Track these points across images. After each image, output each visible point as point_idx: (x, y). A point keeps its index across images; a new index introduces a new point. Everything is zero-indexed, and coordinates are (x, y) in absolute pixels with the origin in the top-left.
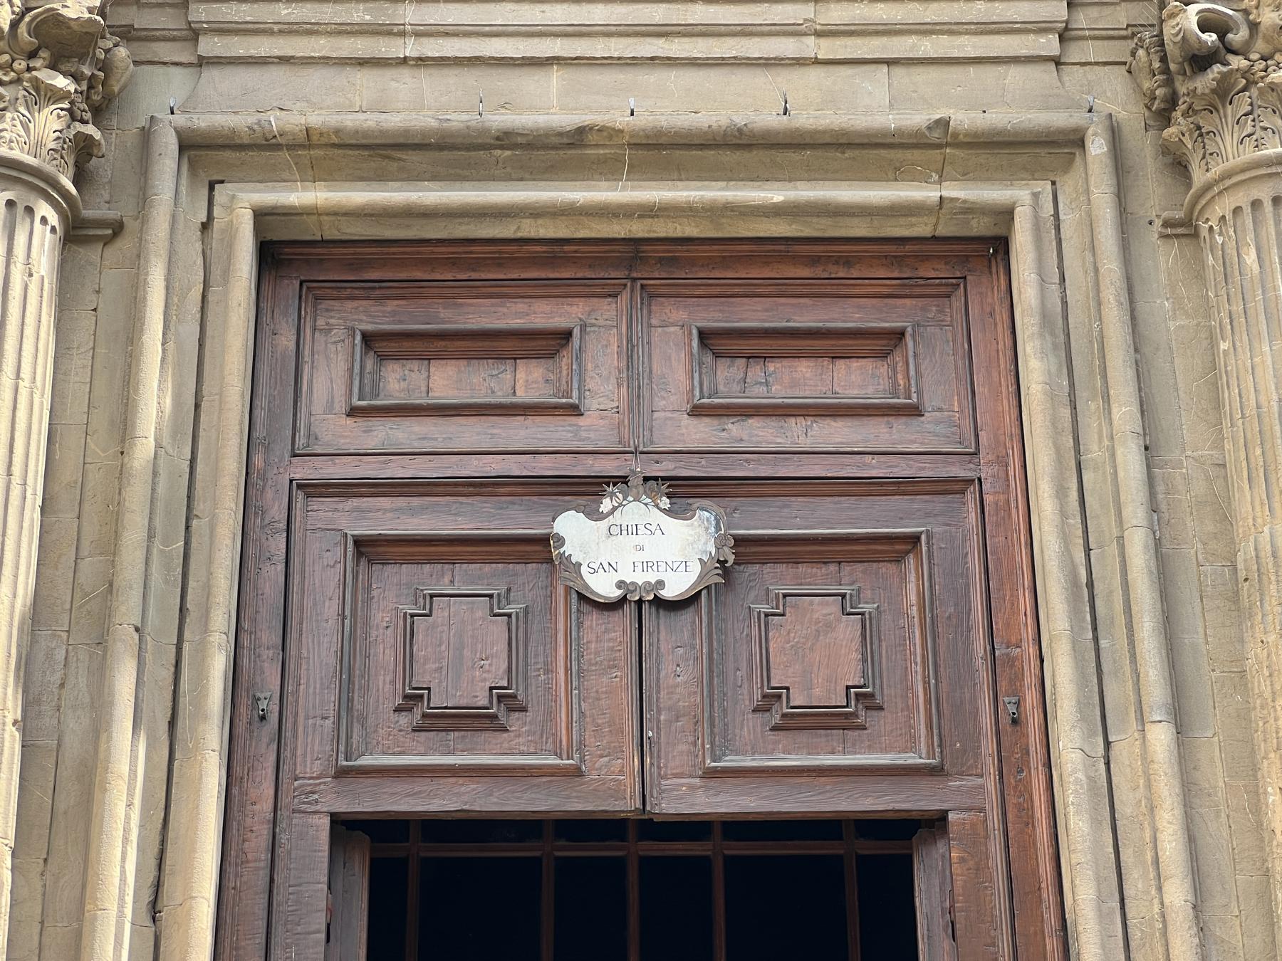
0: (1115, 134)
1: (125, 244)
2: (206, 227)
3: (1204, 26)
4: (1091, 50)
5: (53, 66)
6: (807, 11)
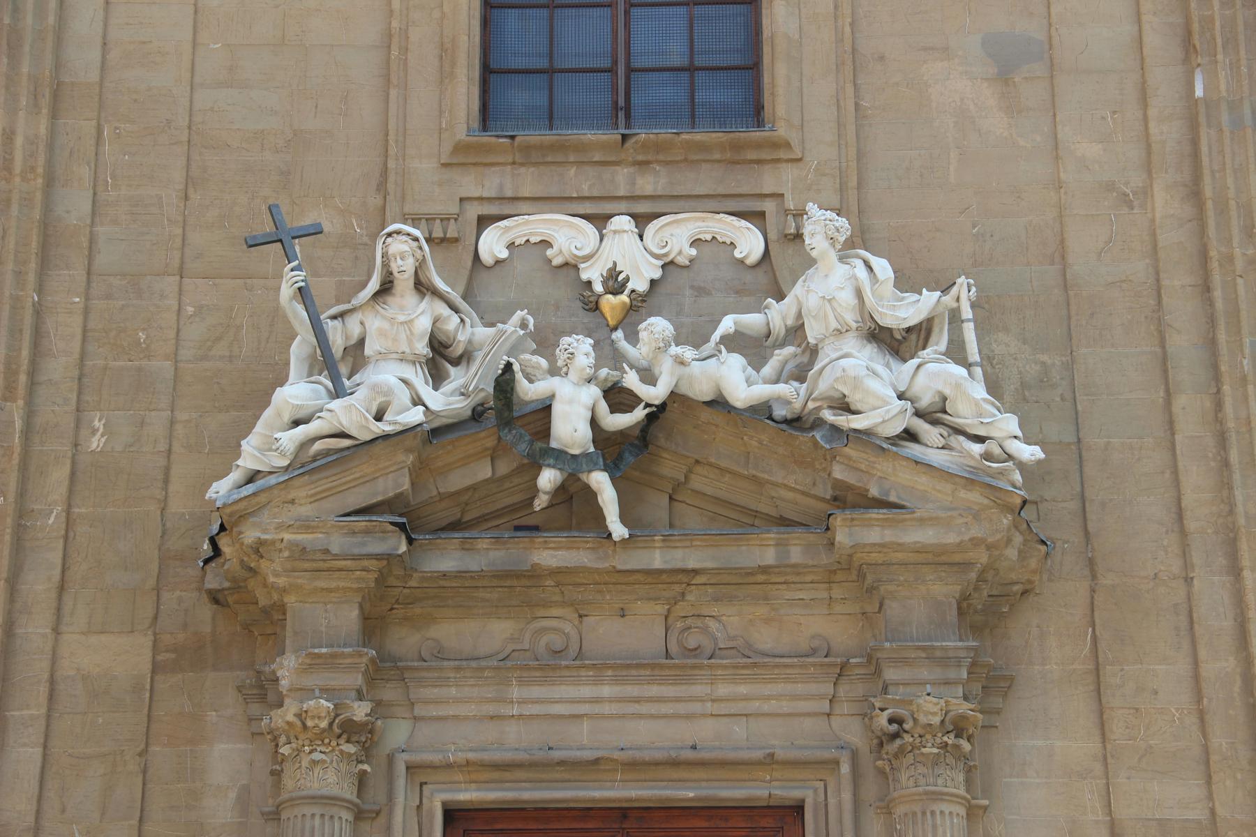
0: (855, 756)
1: (382, 820)
2: (419, 807)
3: (891, 721)
5: (348, 741)
6: (707, 689)
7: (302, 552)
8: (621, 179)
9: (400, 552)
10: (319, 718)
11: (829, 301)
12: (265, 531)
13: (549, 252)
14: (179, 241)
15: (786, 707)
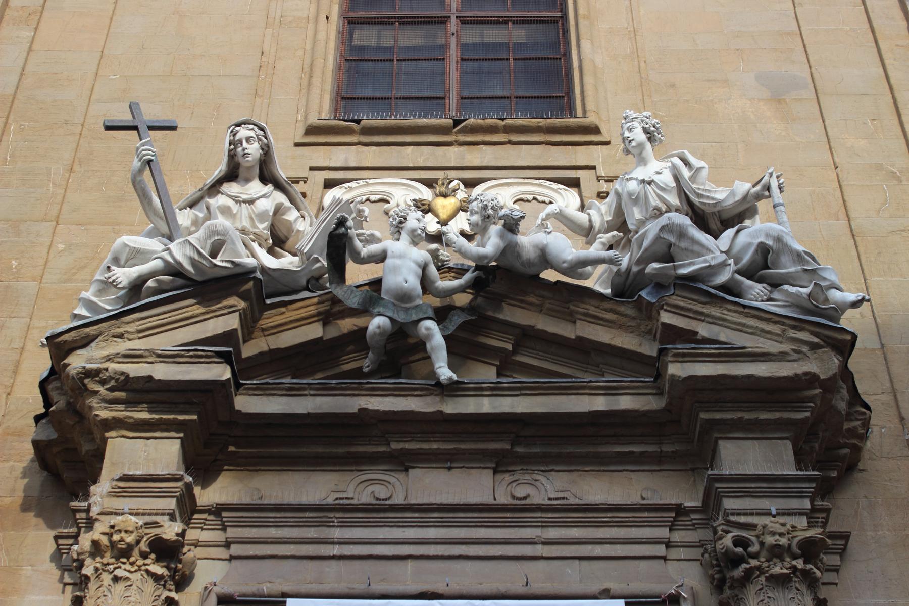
0: (694, 596)
4: (682, 553)
7: (126, 383)
8: (452, 155)
9: (224, 378)
10: (126, 532)
11: (650, 183)
12: (90, 361)
13: (387, 206)
14: (59, 199)
15: (619, 550)
